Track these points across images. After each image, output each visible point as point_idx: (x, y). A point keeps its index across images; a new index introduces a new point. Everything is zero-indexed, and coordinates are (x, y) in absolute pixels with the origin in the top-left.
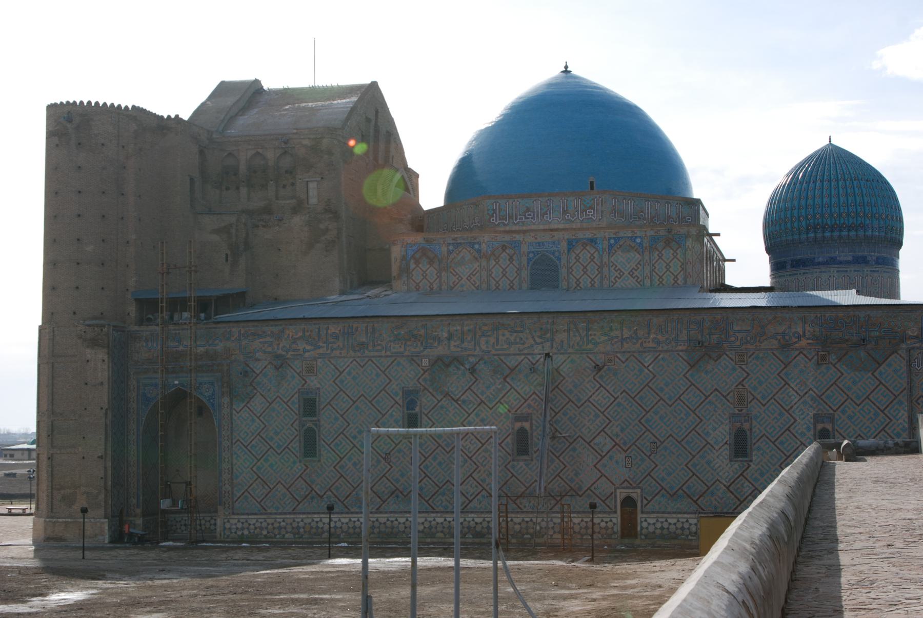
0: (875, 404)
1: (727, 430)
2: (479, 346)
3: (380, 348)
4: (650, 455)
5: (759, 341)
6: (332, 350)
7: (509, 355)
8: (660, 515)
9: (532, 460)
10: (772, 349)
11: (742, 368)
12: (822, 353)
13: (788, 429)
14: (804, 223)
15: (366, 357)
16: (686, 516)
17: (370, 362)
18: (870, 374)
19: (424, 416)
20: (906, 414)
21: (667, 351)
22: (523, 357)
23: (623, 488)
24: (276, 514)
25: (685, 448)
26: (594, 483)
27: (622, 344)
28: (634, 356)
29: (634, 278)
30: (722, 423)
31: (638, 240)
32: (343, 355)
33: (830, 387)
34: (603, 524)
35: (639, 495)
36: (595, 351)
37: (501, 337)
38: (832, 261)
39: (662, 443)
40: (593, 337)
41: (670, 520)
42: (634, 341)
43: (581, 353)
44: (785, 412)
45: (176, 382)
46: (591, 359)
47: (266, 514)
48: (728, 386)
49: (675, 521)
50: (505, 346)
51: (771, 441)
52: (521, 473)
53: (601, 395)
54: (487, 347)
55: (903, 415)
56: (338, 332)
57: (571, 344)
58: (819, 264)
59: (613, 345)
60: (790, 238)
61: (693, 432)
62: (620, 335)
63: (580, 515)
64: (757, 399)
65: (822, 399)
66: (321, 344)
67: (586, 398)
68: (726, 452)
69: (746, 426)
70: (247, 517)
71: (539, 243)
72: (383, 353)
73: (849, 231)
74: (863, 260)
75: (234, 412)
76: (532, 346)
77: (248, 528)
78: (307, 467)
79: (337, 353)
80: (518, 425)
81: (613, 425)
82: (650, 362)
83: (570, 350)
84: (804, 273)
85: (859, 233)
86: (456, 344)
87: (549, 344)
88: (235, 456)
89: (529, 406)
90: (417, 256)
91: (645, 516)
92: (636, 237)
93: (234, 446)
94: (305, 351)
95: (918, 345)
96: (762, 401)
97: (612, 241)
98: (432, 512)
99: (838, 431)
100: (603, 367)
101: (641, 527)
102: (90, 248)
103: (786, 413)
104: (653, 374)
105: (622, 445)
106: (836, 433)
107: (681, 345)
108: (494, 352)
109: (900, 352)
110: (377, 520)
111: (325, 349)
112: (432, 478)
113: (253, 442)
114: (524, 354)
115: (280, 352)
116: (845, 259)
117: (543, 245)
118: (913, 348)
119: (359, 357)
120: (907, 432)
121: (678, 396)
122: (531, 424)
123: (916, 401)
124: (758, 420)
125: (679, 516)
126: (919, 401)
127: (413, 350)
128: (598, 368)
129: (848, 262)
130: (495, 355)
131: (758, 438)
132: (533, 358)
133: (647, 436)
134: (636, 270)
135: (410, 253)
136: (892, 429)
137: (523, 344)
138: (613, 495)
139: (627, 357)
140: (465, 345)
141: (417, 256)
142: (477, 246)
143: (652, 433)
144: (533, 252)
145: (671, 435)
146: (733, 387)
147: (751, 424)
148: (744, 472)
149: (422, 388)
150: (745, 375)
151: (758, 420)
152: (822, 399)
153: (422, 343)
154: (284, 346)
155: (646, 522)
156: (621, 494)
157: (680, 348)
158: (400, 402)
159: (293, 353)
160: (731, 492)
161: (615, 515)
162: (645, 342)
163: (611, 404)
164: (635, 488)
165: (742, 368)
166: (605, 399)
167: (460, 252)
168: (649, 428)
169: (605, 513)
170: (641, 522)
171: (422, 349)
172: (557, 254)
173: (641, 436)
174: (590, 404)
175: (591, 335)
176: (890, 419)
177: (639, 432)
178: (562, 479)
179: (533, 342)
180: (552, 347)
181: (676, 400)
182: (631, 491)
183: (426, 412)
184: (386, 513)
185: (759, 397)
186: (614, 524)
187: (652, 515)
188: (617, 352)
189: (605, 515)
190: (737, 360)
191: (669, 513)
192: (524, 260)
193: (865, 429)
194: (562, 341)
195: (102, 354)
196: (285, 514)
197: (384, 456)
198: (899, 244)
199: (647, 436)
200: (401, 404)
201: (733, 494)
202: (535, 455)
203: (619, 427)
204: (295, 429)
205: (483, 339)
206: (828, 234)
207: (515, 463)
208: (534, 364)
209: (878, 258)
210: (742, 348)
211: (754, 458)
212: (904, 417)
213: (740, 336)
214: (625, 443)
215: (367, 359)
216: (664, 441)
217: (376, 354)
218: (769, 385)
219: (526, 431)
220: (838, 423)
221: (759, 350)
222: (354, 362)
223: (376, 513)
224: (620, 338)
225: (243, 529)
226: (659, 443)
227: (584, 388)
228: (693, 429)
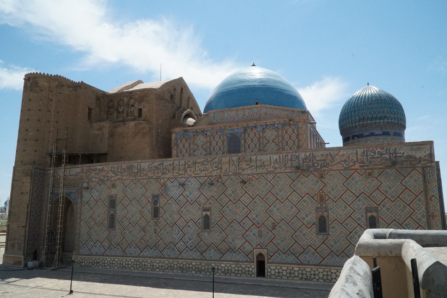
0: (403, 201)
1: (315, 217)
2: (187, 173)
3: (143, 175)
4: (272, 230)
5: (331, 165)
6: (123, 176)
7: (201, 176)
8: (277, 265)
9: (211, 232)
10: (338, 170)
11: (322, 181)
12: (369, 171)
13: (350, 216)
14: (357, 118)
15: (137, 179)
16: (292, 266)
17: (138, 182)
18: (399, 183)
19: (161, 208)
20: (424, 207)
21: (281, 173)
22: (207, 177)
23: (257, 248)
24: (96, 256)
25: (291, 226)
26: (242, 245)
27: (257, 170)
28: (262, 176)
29: (274, 143)
30: (311, 212)
31: (276, 125)
32: (127, 179)
33: (375, 191)
34: (247, 269)
35: (266, 252)
36: (243, 174)
37: (197, 168)
38: (372, 134)
39: (278, 223)
40: (241, 166)
41: (283, 268)
42: (263, 167)
43: (236, 175)
44: (347, 206)
46: (240, 178)
48: (314, 191)
49: (286, 268)
50: (199, 172)
51: (340, 223)
52: (205, 238)
53: (246, 197)
54: (190, 173)
55: (422, 207)
56: (125, 167)
57: (231, 170)
58: (366, 136)
59: (252, 170)
60: (351, 125)
61: (295, 217)
62: (255, 165)
63: (235, 263)
64: (331, 199)
65: (370, 198)
66: (118, 173)
67: (238, 199)
68: (314, 229)
69: (325, 214)
70: (83, 256)
71: (232, 129)
72: (144, 177)
73: (380, 120)
74: (387, 134)
75: (82, 206)
76: (212, 171)
77: (84, 262)
78: (110, 233)
79: (125, 178)
80: (204, 213)
81: (252, 213)
82: (271, 178)
83: (231, 173)
84: (358, 141)
85: (385, 121)
86: (176, 172)
87: (220, 170)
88: (81, 227)
89: (210, 203)
90: (181, 138)
91: (269, 265)
92: (275, 124)
93: (81, 222)
94: (112, 177)
95: (429, 164)
96: (334, 200)
97: (264, 127)
98: (163, 258)
99: (380, 217)
100: (247, 182)
101: (267, 271)
102: (31, 134)
103: (348, 207)
104: (273, 185)
105: (256, 225)
106: (380, 219)
107: (287, 169)
108: (193, 175)
109: (417, 169)
110: (138, 261)
111: (120, 176)
112: (164, 240)
114: (208, 176)
115: (102, 178)
116: (378, 133)
117: (234, 130)
118: (426, 167)
119: (134, 179)
120: (425, 218)
121: (286, 197)
122: (211, 213)
123: (430, 199)
124: (332, 211)
125: (288, 266)
126: (432, 199)
127: (157, 175)
128: (244, 182)
129: (380, 135)
130: (194, 177)
131: (332, 221)
132: (212, 178)
133: (270, 219)
134: (275, 139)
135: (178, 137)
136: (416, 216)
137: (207, 171)
138: (252, 252)
139: (259, 177)
140: (181, 172)
141: (181, 138)
142: (205, 132)
143: (273, 218)
144: (229, 134)
145: (283, 219)
146: (317, 192)
147: (328, 213)
148: (324, 241)
149: (161, 194)
150: (324, 185)
151: (332, 211)
152: (370, 198)
153: (161, 172)
154: (104, 175)
155: (270, 268)
156: (256, 252)
157: (288, 171)
158: (151, 201)
160: (318, 253)
161: (253, 264)
162: (269, 168)
163: (251, 202)
164: (263, 249)
165: (322, 181)
166: (248, 199)
167: (198, 135)
168: (271, 215)
169: (248, 262)
170: (267, 268)
171: (161, 175)
172: (239, 134)
173: (267, 220)
174: (240, 202)
175: (241, 165)
176: (413, 210)
177: (266, 217)
178: (226, 242)
179: (211, 169)
180: (221, 172)
181: (286, 200)
182: (262, 250)
183: (162, 206)
184: (142, 257)
185: (332, 197)
186: (253, 269)
187: (274, 265)
188: (254, 174)
189: (248, 264)
190: (319, 177)
191: (282, 263)
192: (225, 137)
193: (398, 216)
194: (226, 169)
195: (28, 179)
196: (100, 256)
197: (142, 228)
198: (404, 127)
199: (270, 219)
200: (151, 202)
201: (319, 254)
202: (213, 229)
203: (255, 215)
205: (188, 169)
207: (203, 233)
208: (212, 181)
209: (395, 133)
210: (322, 169)
211: (331, 233)
212: (422, 209)
213: (320, 163)
214: (258, 223)
215: (137, 180)
216: (279, 223)
217: (141, 178)
218: (338, 190)
219: (208, 216)
220: (381, 212)
221: (331, 170)
222: (132, 182)
223: (138, 257)
224: (255, 166)
225: (82, 262)
226: (276, 224)
227: (237, 193)
228: (295, 216)
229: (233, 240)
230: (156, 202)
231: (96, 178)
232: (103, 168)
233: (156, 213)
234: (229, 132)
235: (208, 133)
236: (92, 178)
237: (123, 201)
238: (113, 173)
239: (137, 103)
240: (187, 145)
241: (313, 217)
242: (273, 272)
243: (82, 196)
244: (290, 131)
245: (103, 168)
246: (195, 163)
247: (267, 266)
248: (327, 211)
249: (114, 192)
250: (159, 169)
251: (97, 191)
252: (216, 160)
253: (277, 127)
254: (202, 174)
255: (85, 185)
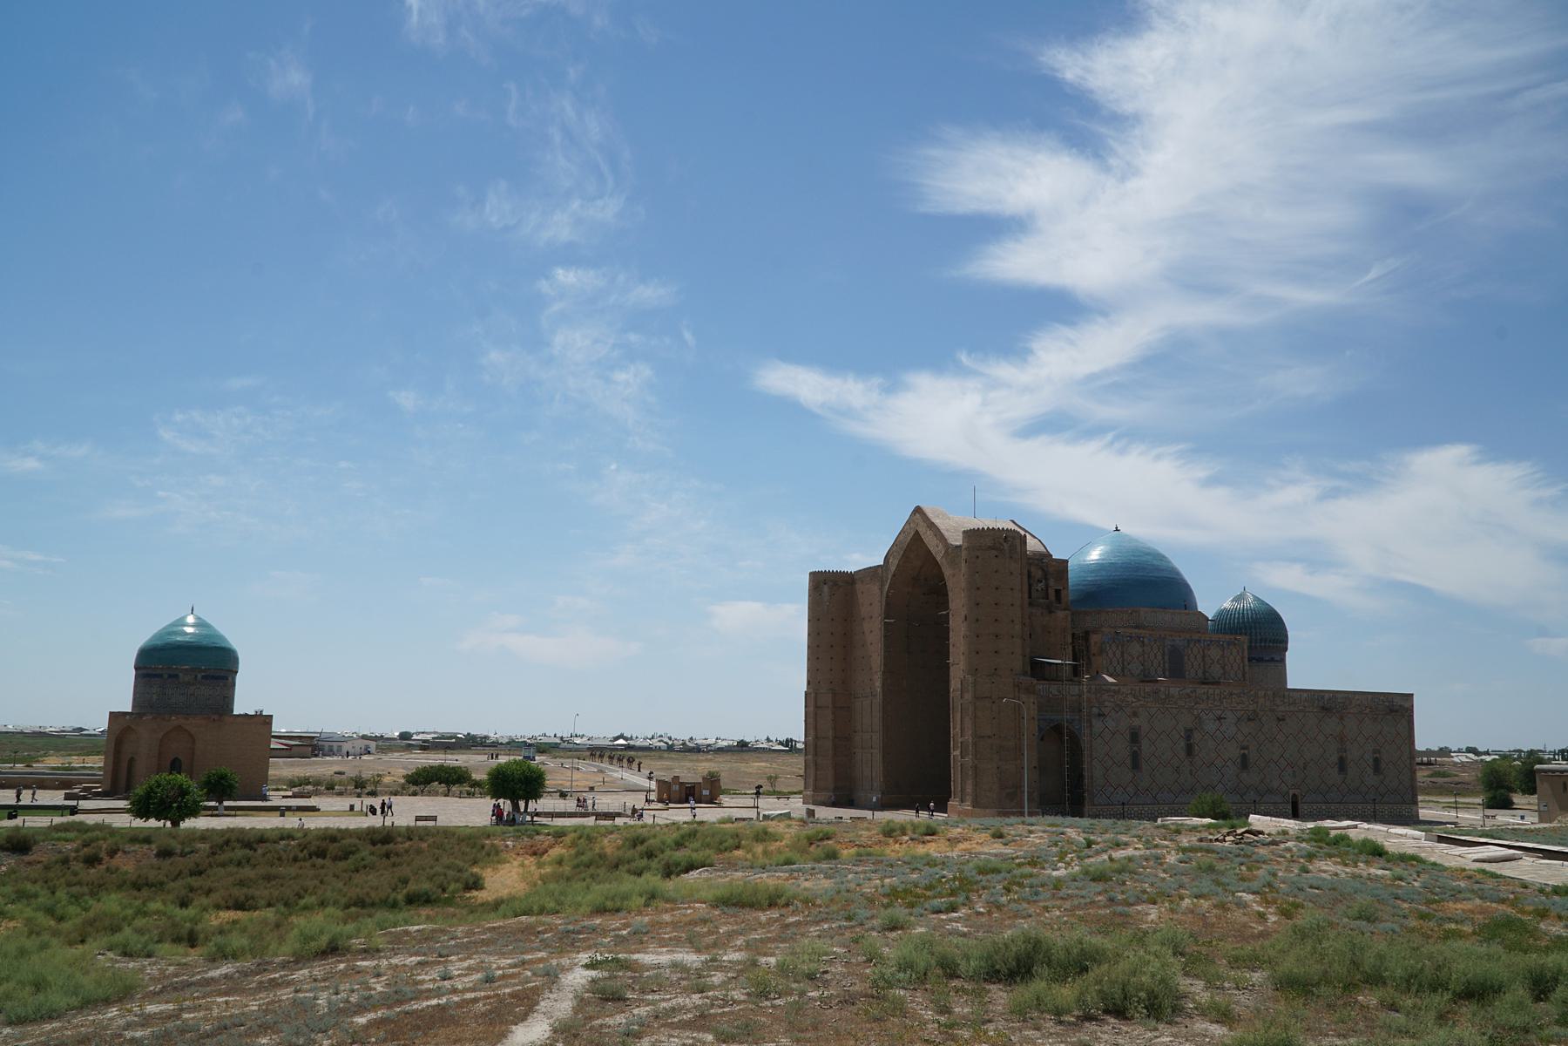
6: (1147, 702)
38: (1272, 660)
68: (1336, 769)
80: (1242, 751)
156: (1291, 792)
198: (1286, 649)
206: (1271, 644)
223: (1174, 804)
229: (1271, 781)
230: (1188, 738)
231: (1110, 701)
232: (1119, 689)
233: (1189, 750)
234: (1169, 643)
235: (1146, 640)
236: (1104, 701)
238: (1134, 696)
239: (1052, 580)
240: (1118, 654)
241: (1334, 758)
242: (1306, 812)
243: (1091, 726)
244: (1235, 651)
245: (1119, 689)
246: (1231, 694)
247: (1300, 806)
248: (1345, 752)
249: (1136, 722)
250: (1190, 697)
251: (1113, 720)
252: (1252, 693)
253: (1223, 645)
254: (1239, 708)
255: (1095, 710)
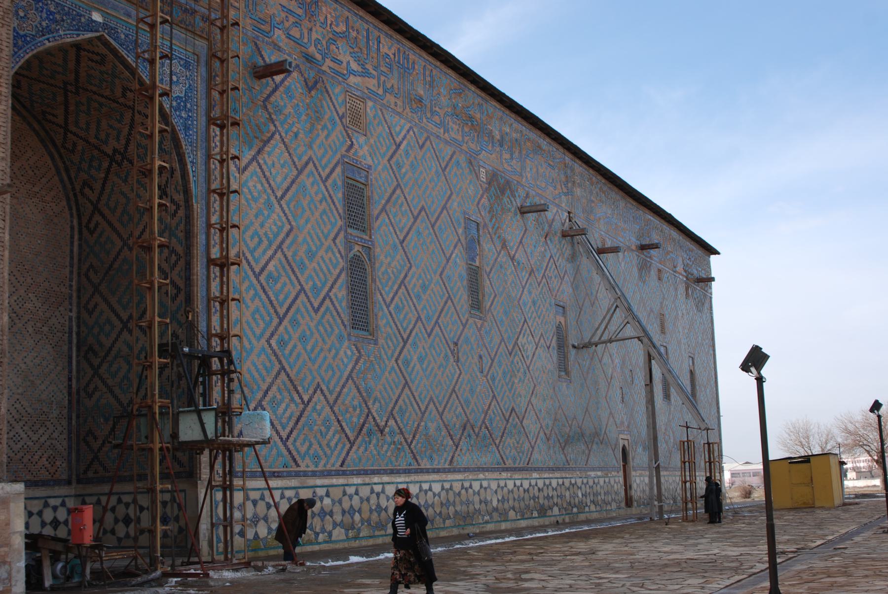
45: (97, 17)
47: (297, 474)
94: (352, 73)
113: (271, 267)
159: (332, 65)
204: (340, 252)
237: (393, 210)
